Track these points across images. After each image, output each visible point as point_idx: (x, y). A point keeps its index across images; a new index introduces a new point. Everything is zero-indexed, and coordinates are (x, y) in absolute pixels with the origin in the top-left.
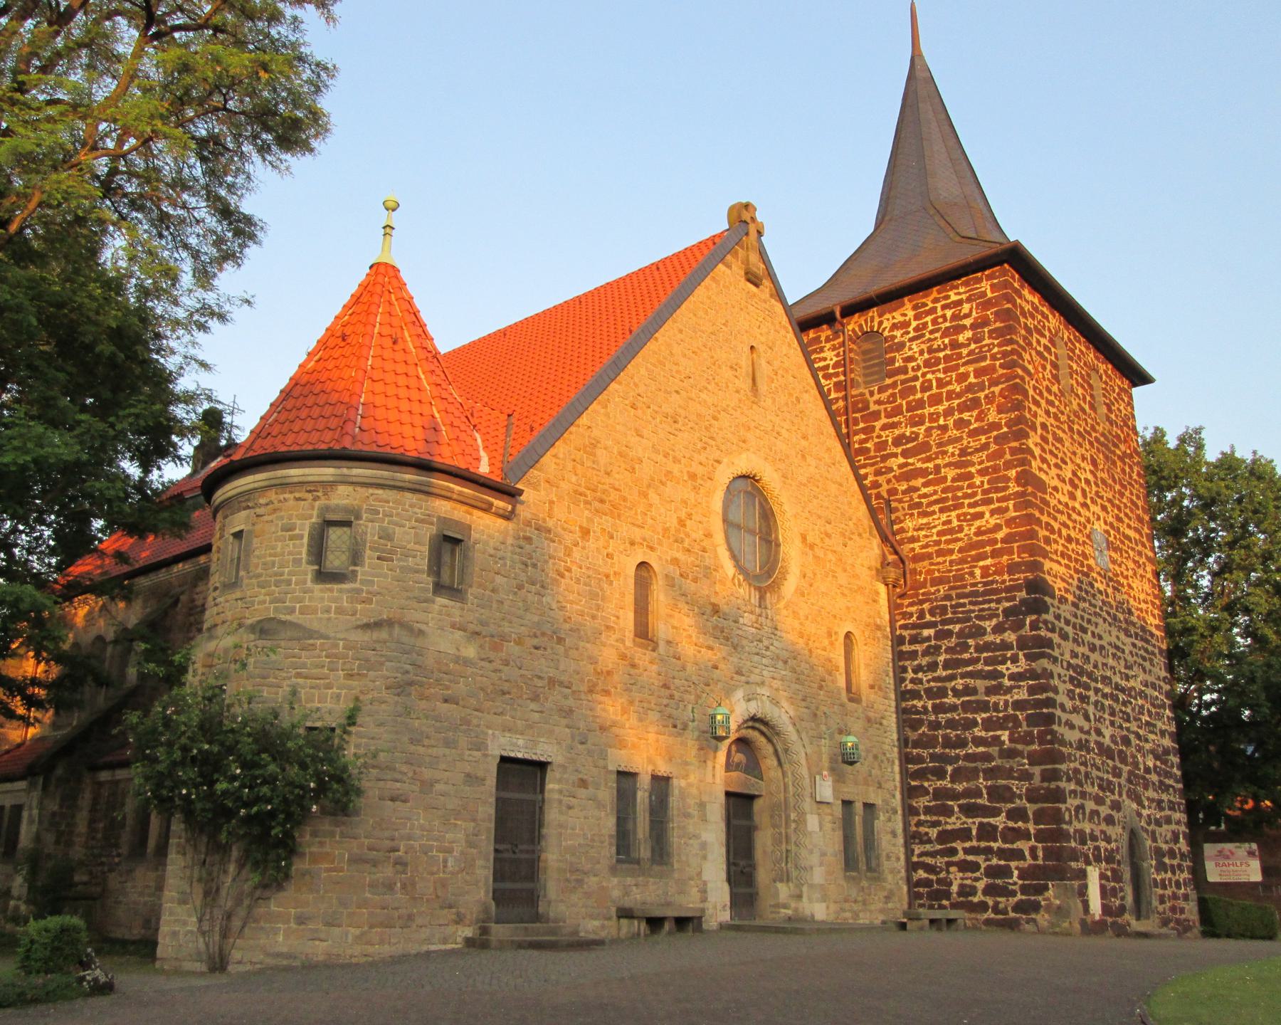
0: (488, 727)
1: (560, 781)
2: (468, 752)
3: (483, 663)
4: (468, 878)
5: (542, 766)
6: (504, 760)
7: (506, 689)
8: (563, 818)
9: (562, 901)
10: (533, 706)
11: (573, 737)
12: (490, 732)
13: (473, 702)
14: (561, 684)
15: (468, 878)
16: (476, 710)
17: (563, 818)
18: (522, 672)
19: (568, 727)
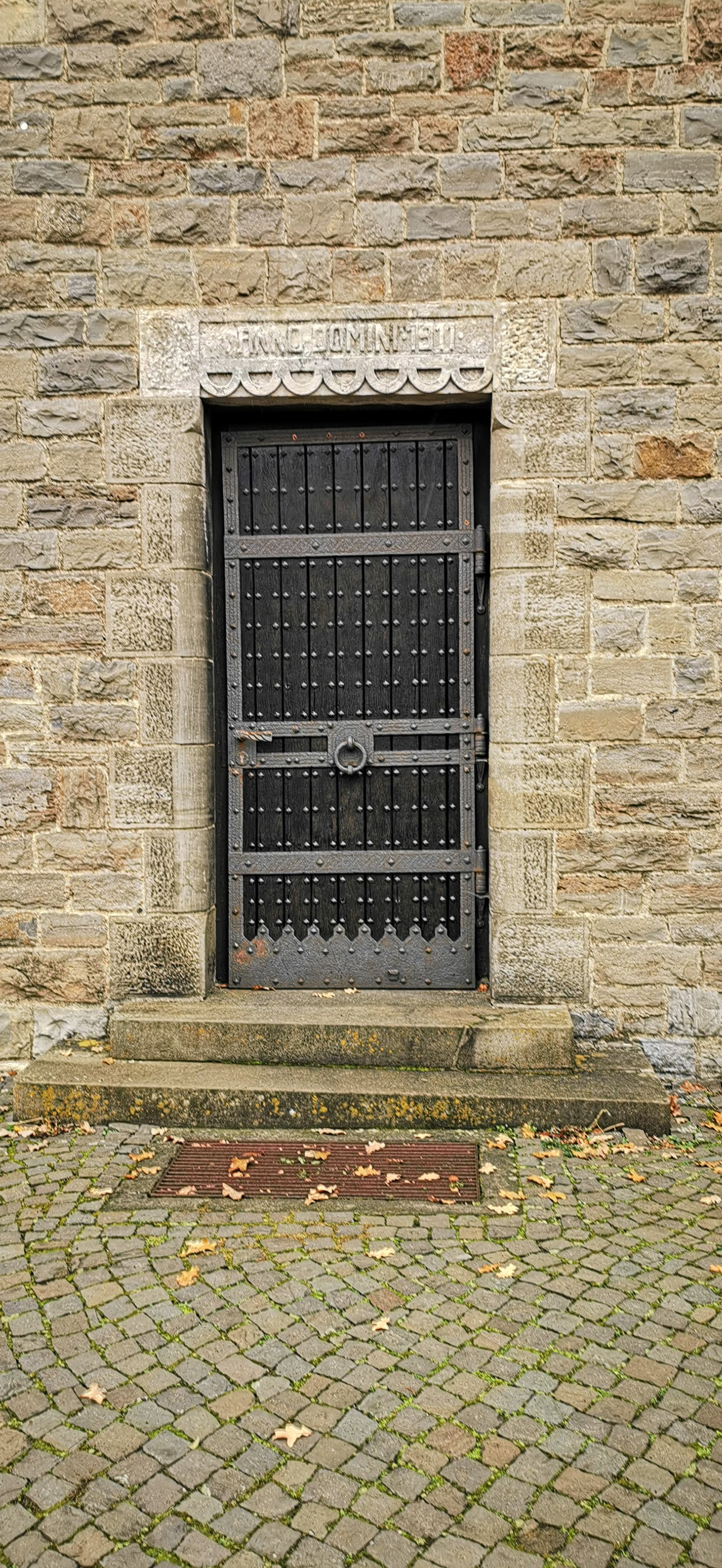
0: (133, 299)
1: (534, 462)
2: (36, 406)
3: (81, 53)
4: (74, 845)
5: (470, 416)
6: (223, 419)
7: (204, 134)
8: (553, 609)
9: (560, 919)
10: (377, 173)
11: (610, 276)
12: (144, 315)
13: (44, 212)
14: (524, 55)
15: (74, 845)
16: (66, 240)
17: (553, 609)
18: (296, 46)
19: (575, 230)
